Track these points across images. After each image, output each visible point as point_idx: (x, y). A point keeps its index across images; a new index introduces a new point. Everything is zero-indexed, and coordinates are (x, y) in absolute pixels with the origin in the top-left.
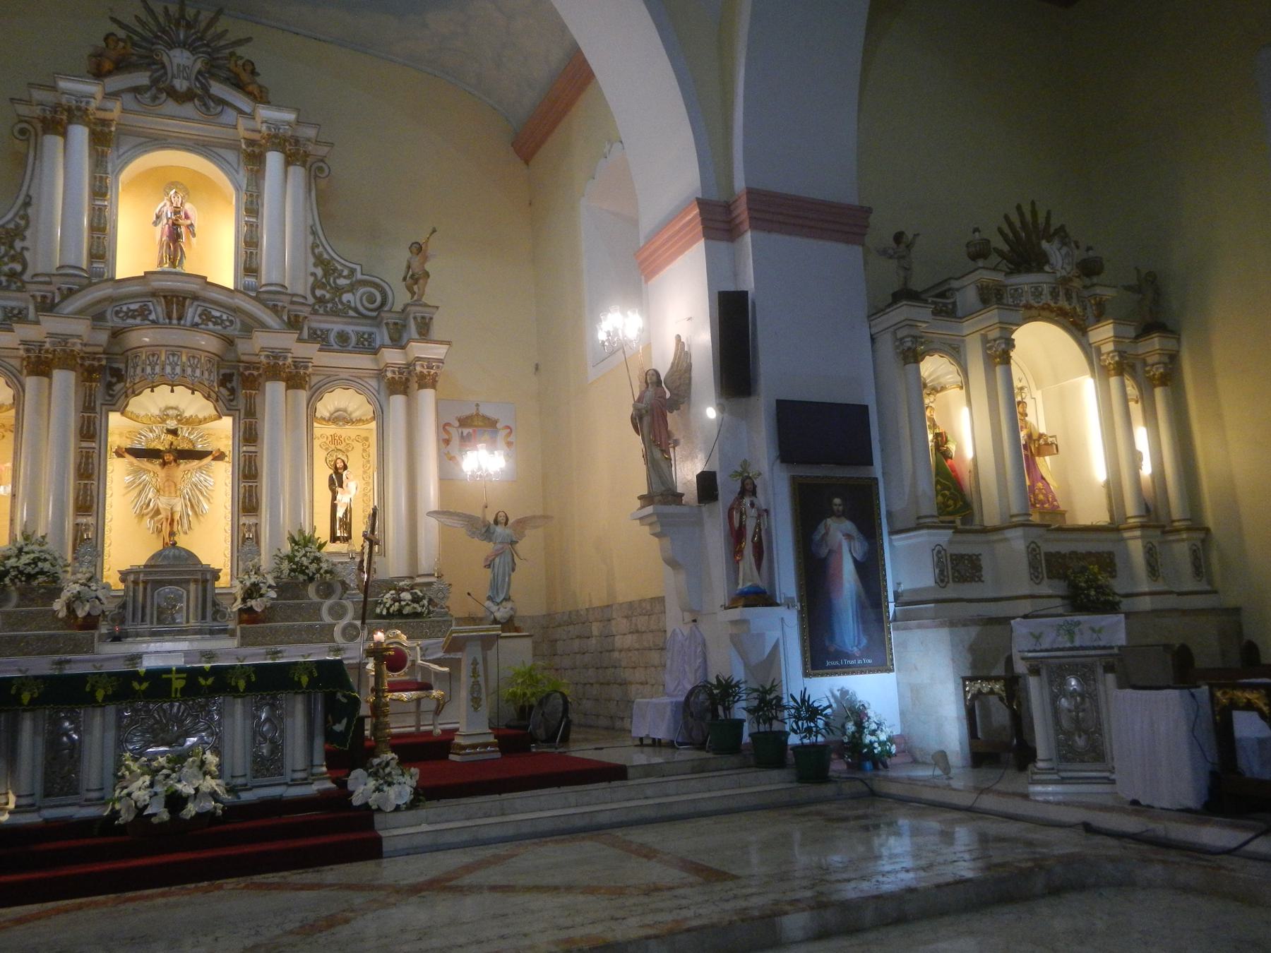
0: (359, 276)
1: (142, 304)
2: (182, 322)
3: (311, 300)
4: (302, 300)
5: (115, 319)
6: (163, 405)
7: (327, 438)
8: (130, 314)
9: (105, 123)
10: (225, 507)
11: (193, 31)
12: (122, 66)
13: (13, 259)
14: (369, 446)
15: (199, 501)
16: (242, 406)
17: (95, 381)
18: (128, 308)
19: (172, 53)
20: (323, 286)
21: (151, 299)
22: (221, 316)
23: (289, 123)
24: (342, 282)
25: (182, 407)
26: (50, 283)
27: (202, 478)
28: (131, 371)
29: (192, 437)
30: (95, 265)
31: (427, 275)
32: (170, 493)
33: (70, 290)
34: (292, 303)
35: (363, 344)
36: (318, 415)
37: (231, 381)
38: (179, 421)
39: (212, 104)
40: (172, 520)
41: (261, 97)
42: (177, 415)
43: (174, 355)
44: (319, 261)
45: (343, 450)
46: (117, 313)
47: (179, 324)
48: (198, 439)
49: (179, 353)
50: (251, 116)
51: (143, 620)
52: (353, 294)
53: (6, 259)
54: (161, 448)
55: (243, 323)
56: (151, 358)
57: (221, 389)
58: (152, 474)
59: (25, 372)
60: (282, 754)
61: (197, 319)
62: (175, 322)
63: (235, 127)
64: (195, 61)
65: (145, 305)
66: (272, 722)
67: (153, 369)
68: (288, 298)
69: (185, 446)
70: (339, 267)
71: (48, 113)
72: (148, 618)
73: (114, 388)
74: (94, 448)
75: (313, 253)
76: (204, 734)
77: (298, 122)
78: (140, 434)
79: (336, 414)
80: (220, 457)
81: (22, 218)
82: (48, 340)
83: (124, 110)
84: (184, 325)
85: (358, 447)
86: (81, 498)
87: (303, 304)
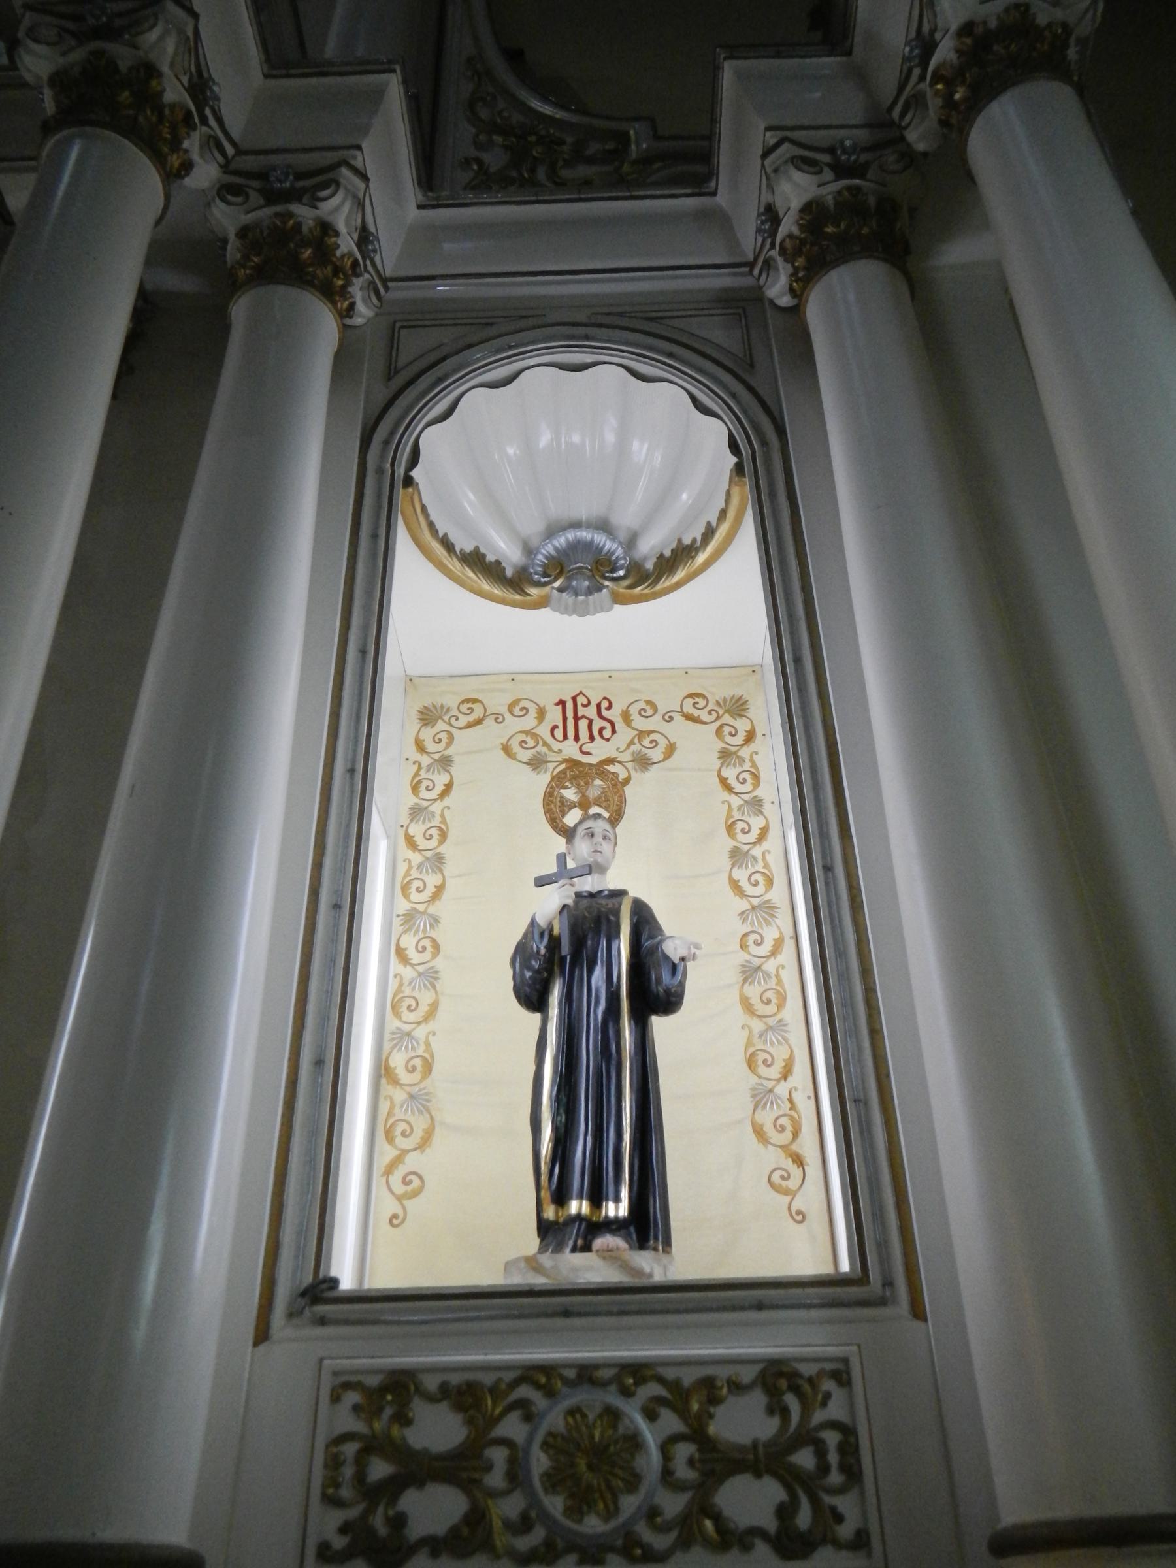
7: (541, 714)
14: (750, 737)
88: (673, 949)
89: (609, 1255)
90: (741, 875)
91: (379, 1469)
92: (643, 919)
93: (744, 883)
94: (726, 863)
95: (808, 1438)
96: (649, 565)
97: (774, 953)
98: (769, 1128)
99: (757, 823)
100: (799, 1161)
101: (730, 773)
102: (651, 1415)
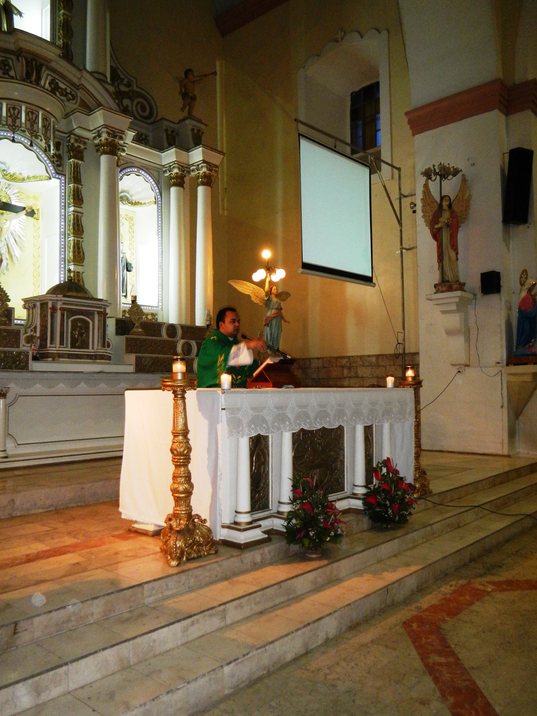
0: (135, 88)
1: (4, 59)
10: (34, 256)
14: (133, 225)
21: (11, 56)
22: (66, 89)
24: (123, 88)
42: (4, 170)
43: (32, 113)
49: (37, 113)
52: (132, 101)
56: (12, 112)
65: (6, 61)
67: (14, 121)
70: (122, 76)
90: (130, 247)
96: (134, 202)
97: (133, 260)
99: (133, 239)
101: (130, 230)
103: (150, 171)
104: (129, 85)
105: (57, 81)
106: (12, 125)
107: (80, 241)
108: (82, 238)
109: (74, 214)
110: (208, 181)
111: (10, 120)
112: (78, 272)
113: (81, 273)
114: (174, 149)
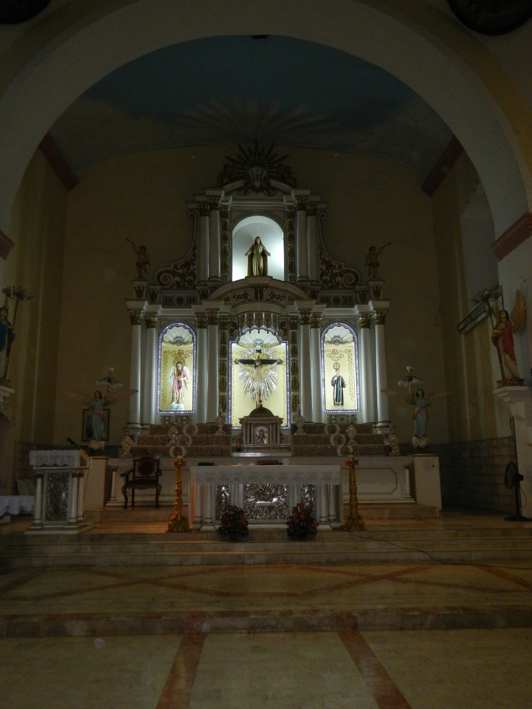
0: (344, 268)
1: (244, 292)
2: (262, 299)
3: (321, 282)
4: (316, 283)
5: (233, 299)
6: (254, 339)
7: (331, 351)
8: (240, 296)
9: (226, 207)
11: (262, 157)
12: (232, 180)
13: (190, 275)
14: (351, 355)
15: (271, 384)
16: (290, 336)
17: (226, 329)
18: (239, 294)
19: (253, 170)
20: (326, 275)
22: (279, 294)
23: (307, 196)
24: (335, 271)
25: (263, 339)
26: (205, 285)
27: (272, 373)
28: (240, 324)
29: (268, 353)
30: (224, 274)
31: (378, 264)
32: (259, 380)
33: (214, 288)
34: (312, 285)
35: (347, 303)
36: (326, 340)
37: (284, 326)
38: (262, 346)
39: (271, 190)
40: (260, 394)
41: (294, 186)
42: (261, 343)
43: (259, 315)
44: (324, 262)
45: (339, 357)
46: (234, 297)
47: (261, 300)
48: (270, 354)
50: (288, 194)
51: (250, 442)
53: (187, 275)
54: (254, 359)
55: (289, 297)
56: (249, 317)
57: (281, 330)
58: (250, 371)
59: (197, 326)
60: (315, 509)
61: (269, 297)
62: (259, 299)
63: (282, 200)
64: (263, 171)
66: (310, 494)
67: (250, 322)
68: (310, 283)
69: (264, 358)
70: (334, 264)
71: (202, 206)
72: (252, 441)
73: (234, 332)
74: (226, 360)
75: (321, 258)
76: (280, 497)
77: (312, 194)
78: (245, 353)
79: (335, 339)
80: (280, 362)
81: (193, 255)
82: (205, 312)
83: (234, 200)
84: (263, 301)
85: (346, 355)
86: (221, 384)
87: (317, 285)
88: (345, 384)
89: (340, 406)
90: (349, 370)
91: (330, 419)
92: (342, 380)
93: (350, 371)
94: (348, 369)
95: (354, 418)
96: (344, 342)
97: (352, 378)
98: (351, 394)
99: (351, 364)
100: (353, 397)
101: (349, 359)
102: (345, 417)
103: (349, 321)
104: (339, 268)
105: (274, 292)
106: (249, 324)
107: (296, 377)
108: (298, 375)
109: (292, 362)
110: (382, 321)
111: (248, 322)
112: (295, 396)
113: (297, 396)
114: (356, 306)
